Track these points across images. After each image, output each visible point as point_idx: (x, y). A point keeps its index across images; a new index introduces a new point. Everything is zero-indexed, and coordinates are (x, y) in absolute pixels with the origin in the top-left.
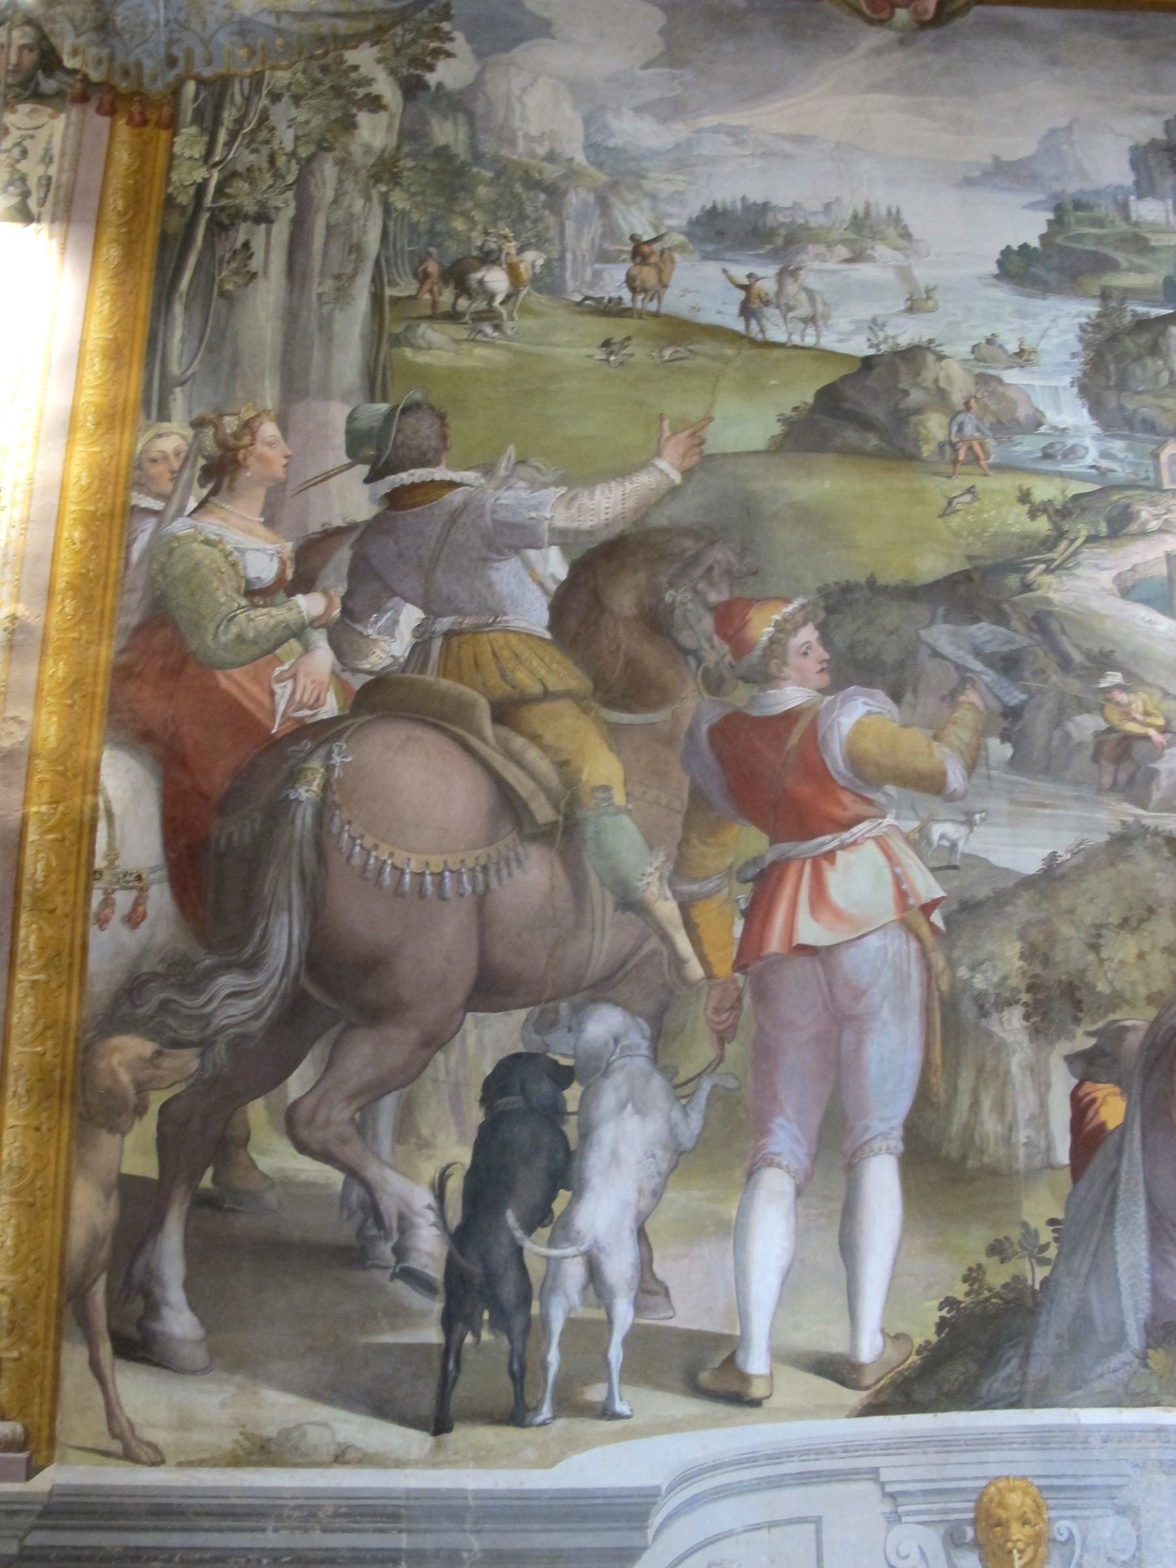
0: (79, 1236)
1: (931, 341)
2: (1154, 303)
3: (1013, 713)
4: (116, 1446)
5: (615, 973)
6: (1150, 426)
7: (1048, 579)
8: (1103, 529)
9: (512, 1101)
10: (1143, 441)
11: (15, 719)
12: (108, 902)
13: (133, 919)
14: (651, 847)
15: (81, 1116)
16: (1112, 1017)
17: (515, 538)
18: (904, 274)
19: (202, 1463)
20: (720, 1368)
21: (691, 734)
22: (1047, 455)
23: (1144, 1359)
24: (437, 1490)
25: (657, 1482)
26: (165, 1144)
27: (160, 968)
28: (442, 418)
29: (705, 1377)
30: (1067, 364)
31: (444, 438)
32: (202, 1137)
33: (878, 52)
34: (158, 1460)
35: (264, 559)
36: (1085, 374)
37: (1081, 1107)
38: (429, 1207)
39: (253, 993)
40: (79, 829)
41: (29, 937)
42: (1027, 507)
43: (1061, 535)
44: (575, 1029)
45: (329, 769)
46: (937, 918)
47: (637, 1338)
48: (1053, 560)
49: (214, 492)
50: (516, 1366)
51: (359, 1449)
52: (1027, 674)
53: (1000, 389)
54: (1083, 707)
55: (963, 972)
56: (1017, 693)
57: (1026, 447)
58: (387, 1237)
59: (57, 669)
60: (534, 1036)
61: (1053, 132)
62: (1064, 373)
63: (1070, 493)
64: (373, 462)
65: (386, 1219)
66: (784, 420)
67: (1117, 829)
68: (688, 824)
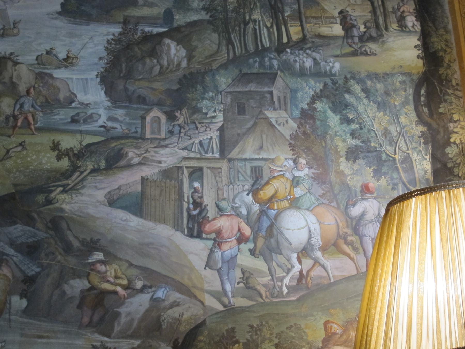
1: (12, 54)
2: (155, 25)
3: (30, 280)
6: (142, 100)
8: (103, 164)
10: (138, 109)
30: (96, 64)
36: (106, 70)
42: (56, 152)
43: (75, 168)
48: (68, 185)
52: (42, 255)
53: (51, 81)
56: (34, 268)
57: (62, 116)
62: (93, 70)
63: (84, 143)
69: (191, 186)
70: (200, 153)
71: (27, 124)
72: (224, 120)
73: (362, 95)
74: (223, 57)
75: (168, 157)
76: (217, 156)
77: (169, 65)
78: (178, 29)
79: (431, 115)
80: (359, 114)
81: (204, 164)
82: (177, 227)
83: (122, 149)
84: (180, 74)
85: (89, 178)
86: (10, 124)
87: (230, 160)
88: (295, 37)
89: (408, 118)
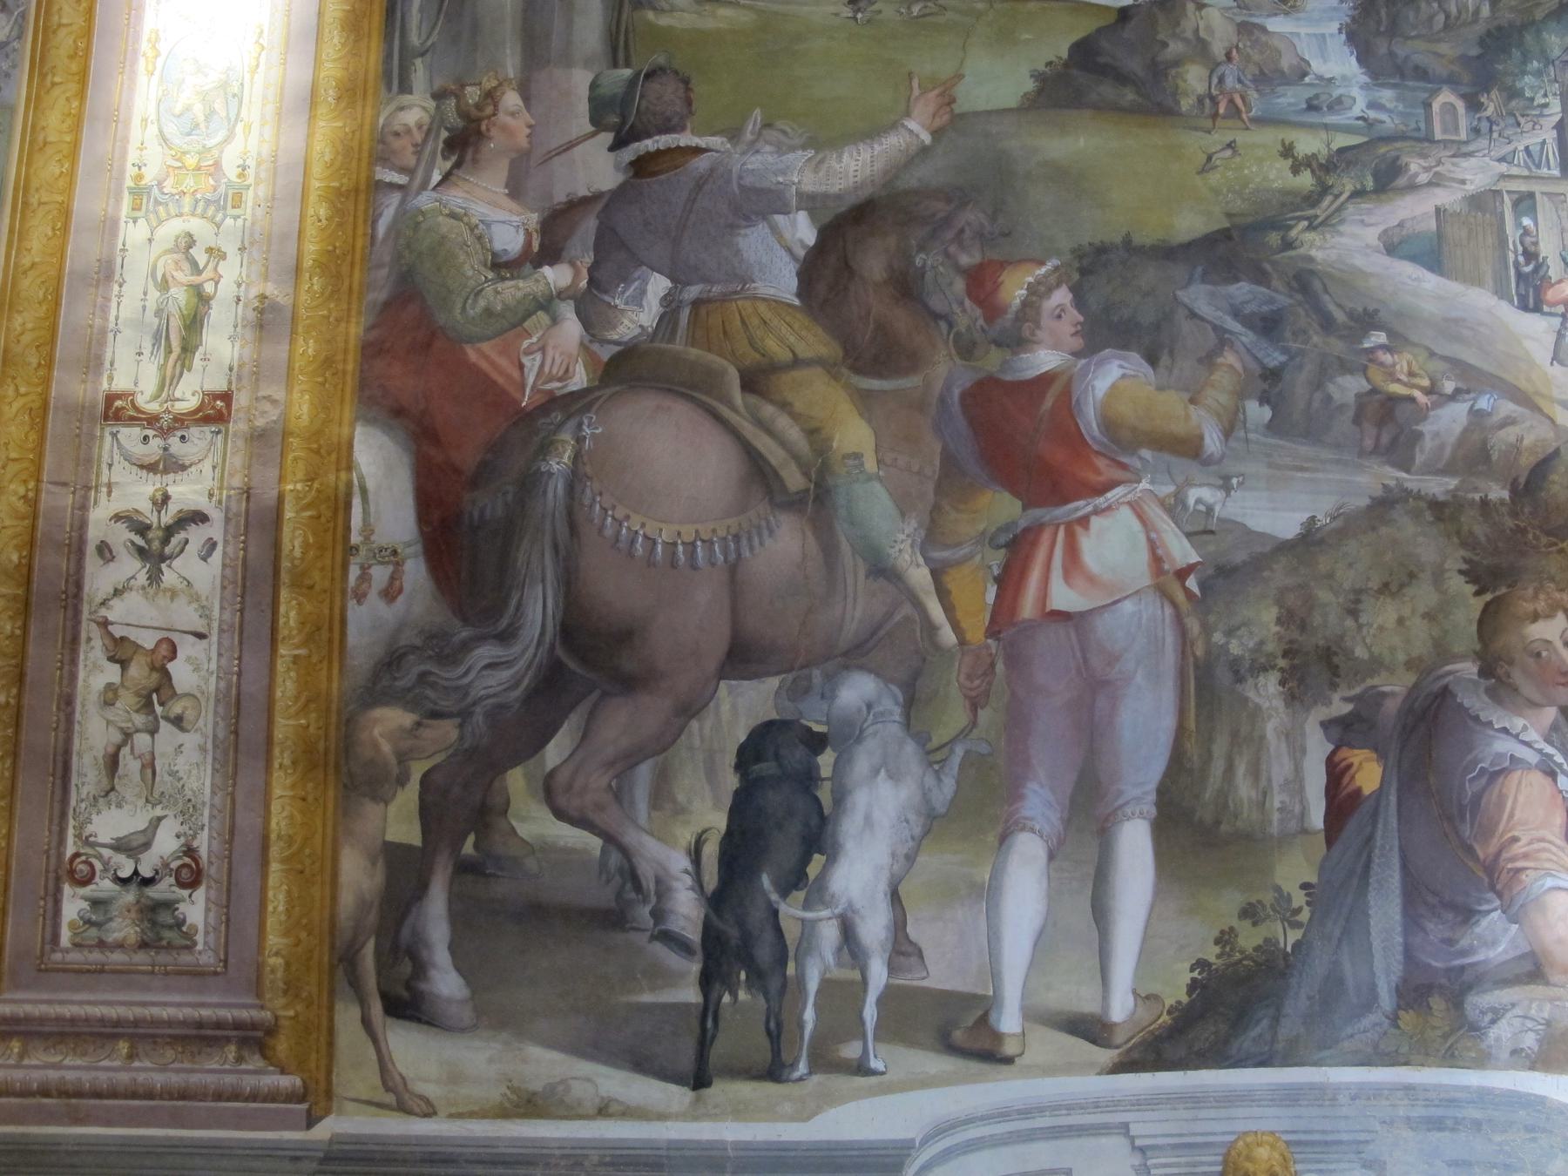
0: (347, 900)
3: (1272, 375)
4: (390, 1099)
5: (867, 641)
6: (1421, 74)
7: (1309, 236)
8: (1370, 183)
9: (767, 768)
10: (1414, 89)
11: (268, 398)
12: (364, 577)
13: (390, 593)
14: (903, 514)
15: (345, 786)
16: (1369, 682)
17: (762, 203)
19: (472, 1115)
20: (971, 1028)
21: (942, 400)
22: (1312, 107)
23: (1394, 1020)
24: (699, 1142)
25: (910, 1135)
26: (426, 813)
27: (418, 642)
28: (686, 82)
29: (958, 1036)
30: (1335, 9)
31: (689, 103)
32: (462, 807)
34: (430, 1112)
35: (510, 230)
36: (1353, 19)
37: (1336, 773)
38: (686, 872)
39: (508, 664)
40: (334, 508)
41: (290, 613)
42: (1290, 161)
43: (1324, 190)
44: (828, 695)
45: (580, 440)
46: (1192, 583)
47: (890, 997)
48: (1317, 217)
49: (458, 165)
50: (772, 1025)
51: (621, 1103)
52: (1288, 334)
53: (1264, 38)
54: (1345, 368)
55: (1218, 637)
56: (1276, 354)
57: (1290, 98)
58: (645, 900)
59: (307, 348)
60: (787, 703)
62: (1331, 19)
63: (1335, 147)
64: (618, 130)
65: (644, 883)
66: (1038, 77)
67: (1378, 492)
68: (938, 489)
69: (1518, 224)
70: (1529, 169)
72: (1563, 111)
76: (1556, 172)
77: (1459, 12)
81: (1537, 188)
82: (1501, 292)
83: (1398, 158)
84: (1480, 28)
85: (1351, 208)
86: (1207, 111)
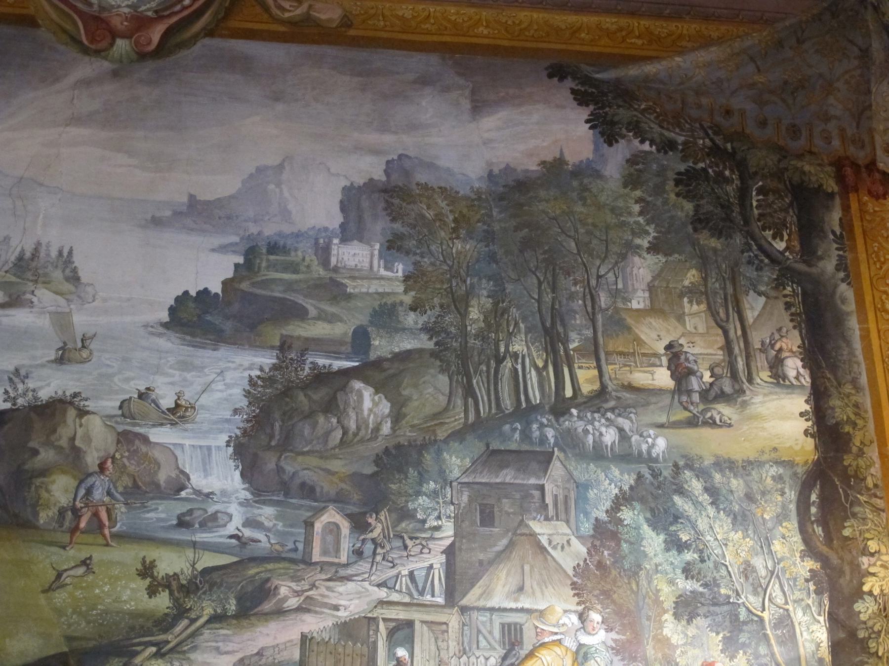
1: (75, 395)
2: (337, 355)
8: (232, 606)
18: (62, 321)
30: (227, 421)
33: (86, 83)
36: (245, 432)
43: (180, 612)
48: (168, 642)
53: (144, 449)
57: (161, 513)
61: (260, 170)
62: (221, 431)
63: (200, 567)
69: (391, 655)
70: (411, 595)
71: (97, 526)
72: (455, 535)
73: (705, 498)
74: (457, 419)
75: (352, 599)
76: (440, 600)
77: (358, 428)
78: (378, 364)
79: (829, 539)
80: (698, 534)
81: (416, 616)
83: (268, 580)
84: (378, 446)
85: (207, 633)
86: (67, 524)
87: (464, 610)
88: (586, 388)
89: (787, 542)
